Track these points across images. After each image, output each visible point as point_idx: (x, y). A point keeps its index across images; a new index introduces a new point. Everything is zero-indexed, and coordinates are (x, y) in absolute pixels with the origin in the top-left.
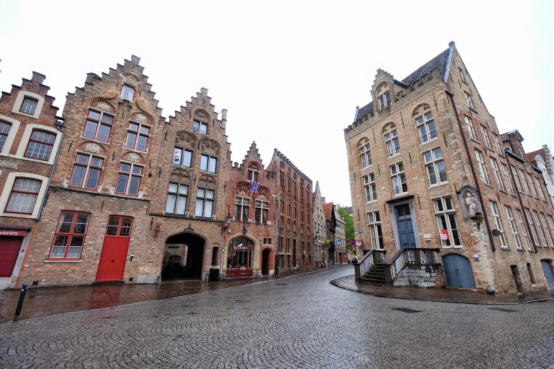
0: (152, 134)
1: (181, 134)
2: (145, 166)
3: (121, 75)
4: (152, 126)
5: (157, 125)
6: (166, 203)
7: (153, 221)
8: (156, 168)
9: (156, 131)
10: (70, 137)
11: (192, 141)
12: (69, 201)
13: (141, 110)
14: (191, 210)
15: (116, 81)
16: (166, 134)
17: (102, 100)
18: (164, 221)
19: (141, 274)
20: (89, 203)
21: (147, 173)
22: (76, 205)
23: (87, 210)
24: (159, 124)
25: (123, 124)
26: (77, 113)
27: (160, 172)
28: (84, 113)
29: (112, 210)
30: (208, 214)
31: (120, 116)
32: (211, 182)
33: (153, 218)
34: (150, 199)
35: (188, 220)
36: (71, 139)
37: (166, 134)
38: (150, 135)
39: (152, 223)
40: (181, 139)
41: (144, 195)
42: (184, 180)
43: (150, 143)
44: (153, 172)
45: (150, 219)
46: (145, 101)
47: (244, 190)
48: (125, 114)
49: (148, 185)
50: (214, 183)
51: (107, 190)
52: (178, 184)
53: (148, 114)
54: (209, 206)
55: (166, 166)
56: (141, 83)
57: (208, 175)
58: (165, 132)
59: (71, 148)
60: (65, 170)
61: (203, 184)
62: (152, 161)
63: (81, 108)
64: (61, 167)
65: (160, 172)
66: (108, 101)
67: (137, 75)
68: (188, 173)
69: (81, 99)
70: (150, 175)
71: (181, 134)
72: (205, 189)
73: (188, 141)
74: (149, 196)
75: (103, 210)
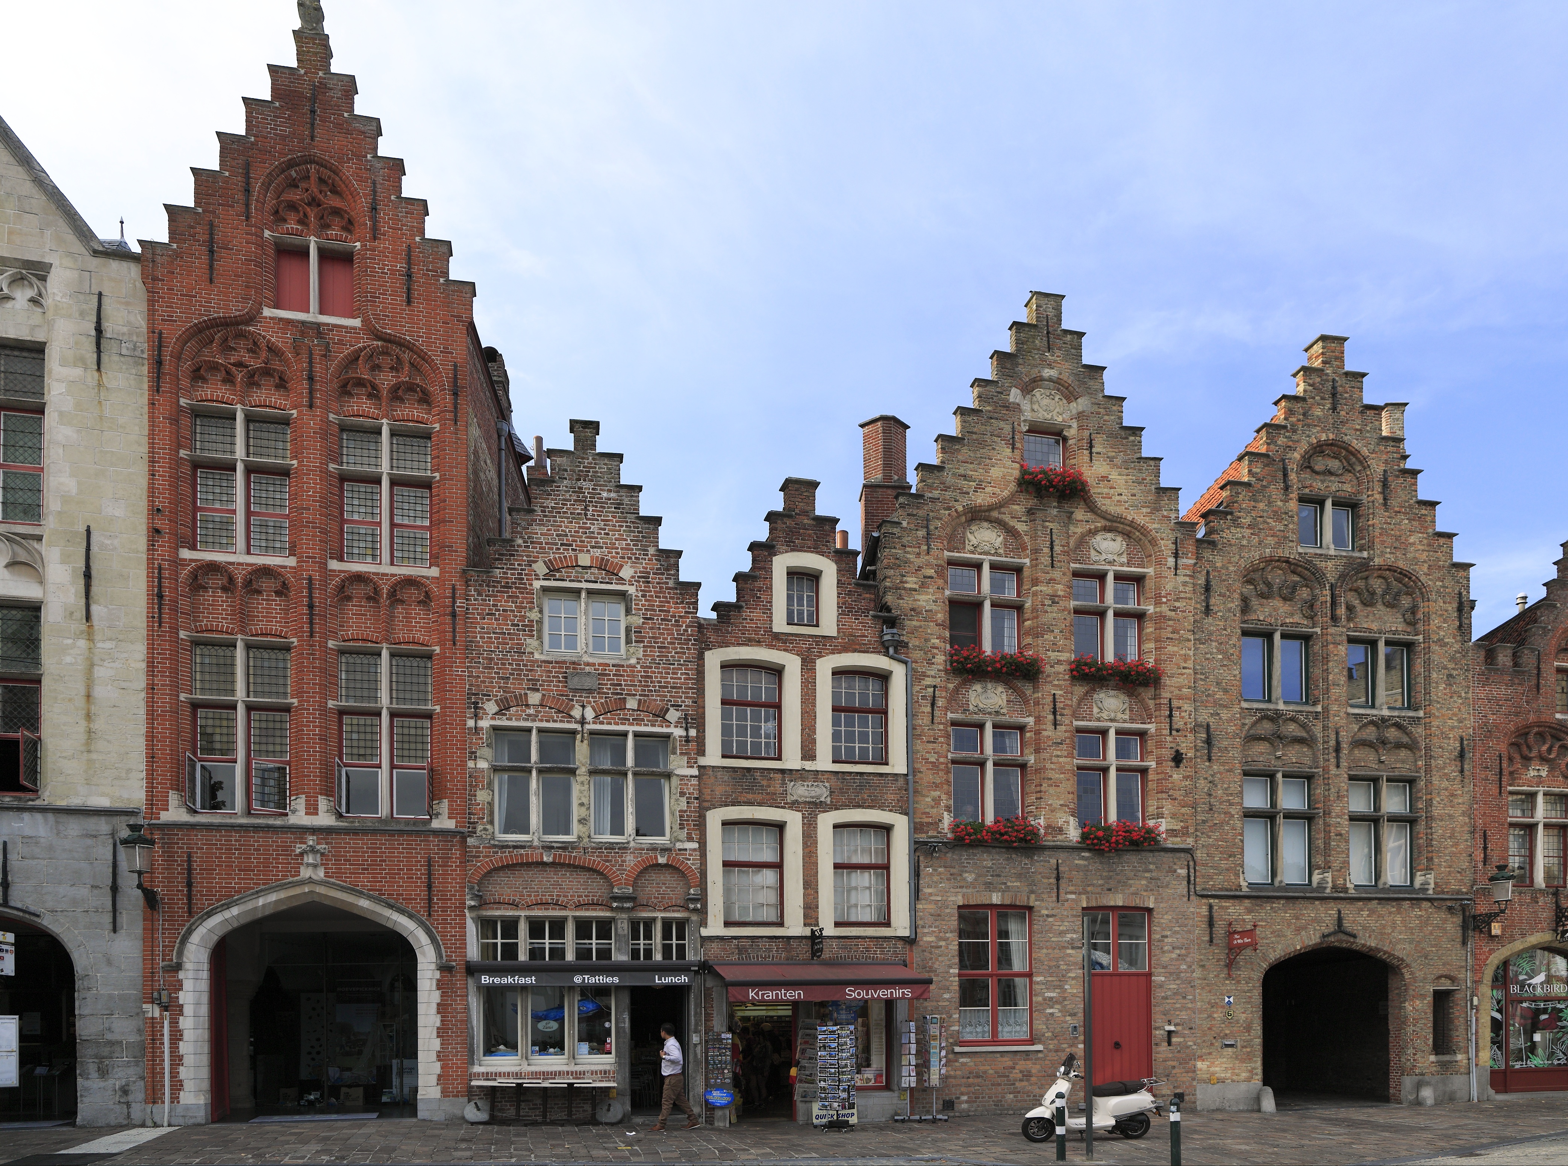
0: (1158, 603)
1: (1257, 576)
2: (1151, 727)
3: (1015, 396)
4: (1150, 571)
5: (1171, 561)
6: (1242, 853)
7: (1215, 915)
8: (1194, 730)
9: (1169, 587)
10: (924, 675)
11: (1304, 593)
12: (970, 877)
13: (1104, 515)
14: (1336, 865)
15: (1007, 428)
16: (1207, 588)
17: (976, 515)
18: (1249, 911)
20: (1019, 876)
21: (1168, 754)
22: (990, 887)
23: (1022, 901)
24: (1176, 555)
25: (1060, 589)
26: (923, 585)
27: (1209, 742)
28: (941, 582)
29: (1085, 892)
30: (1395, 873)
31: (1045, 560)
32: (1399, 746)
33: (1211, 907)
34: (1190, 842)
35: (1332, 904)
36: (928, 681)
37: (1207, 588)
38: (1151, 609)
39: (1211, 923)
40: (1262, 596)
42: (1294, 756)
43: (1157, 640)
44: (1187, 745)
45: (1204, 911)
46: (1114, 475)
47: (1543, 759)
48: (1057, 549)
49: (1177, 794)
50: (1412, 747)
51: (1060, 830)
52: (1272, 776)
53: (1132, 524)
54: (1395, 844)
55: (1225, 715)
56: (1082, 404)
57: (1383, 720)
58: (1202, 581)
59: (937, 713)
60: (936, 786)
61: (1368, 760)
62: (1175, 703)
63: (929, 565)
64: (927, 776)
65: (1209, 742)
66: (995, 514)
67: (1065, 377)
68: (1303, 726)
69: (921, 533)
70: (1178, 759)
71: (1257, 576)
72: (1375, 780)
73: (1285, 599)
74: (1184, 832)
75: (1062, 896)
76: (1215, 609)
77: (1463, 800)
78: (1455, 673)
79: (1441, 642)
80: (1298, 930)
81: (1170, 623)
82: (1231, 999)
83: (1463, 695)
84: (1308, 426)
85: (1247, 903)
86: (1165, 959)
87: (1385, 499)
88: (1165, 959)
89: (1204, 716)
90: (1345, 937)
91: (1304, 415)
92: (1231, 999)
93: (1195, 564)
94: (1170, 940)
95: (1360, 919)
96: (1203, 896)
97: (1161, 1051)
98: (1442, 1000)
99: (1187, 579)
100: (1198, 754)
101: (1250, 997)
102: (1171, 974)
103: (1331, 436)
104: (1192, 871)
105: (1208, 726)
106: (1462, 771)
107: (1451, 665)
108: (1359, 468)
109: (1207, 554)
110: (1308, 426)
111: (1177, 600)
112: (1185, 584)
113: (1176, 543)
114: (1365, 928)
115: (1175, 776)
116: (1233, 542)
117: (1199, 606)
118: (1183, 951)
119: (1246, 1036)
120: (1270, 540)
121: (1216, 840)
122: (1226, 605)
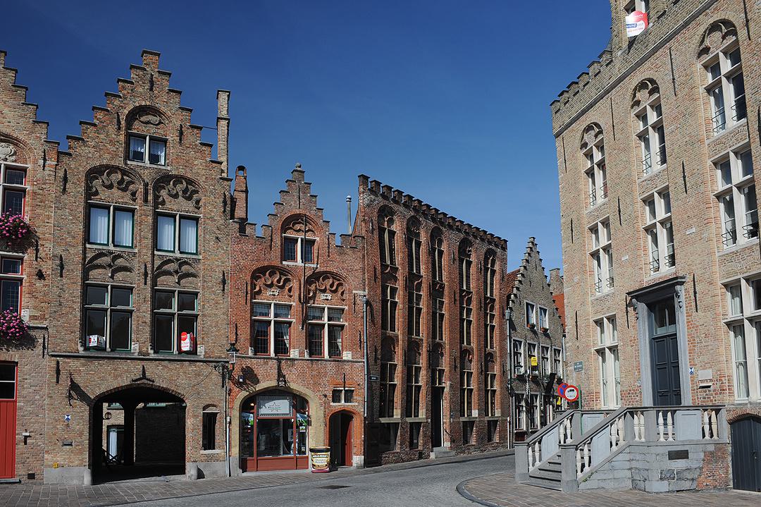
5: (41, 162)
18: (84, 365)
19: (49, 466)
21: (35, 272)
24: (45, 160)
33: (58, 362)
41: (33, 318)
44: (47, 267)
45: (53, 364)
49: (38, 295)
58: (61, 174)
70: (40, 275)
74: (43, 318)
76: (69, 191)
77: (225, 304)
78: (220, 236)
79: (212, 219)
80: (116, 377)
81: (38, 196)
82: (69, 417)
83: (225, 248)
84: (134, 96)
85: (82, 361)
86: (24, 392)
87: (180, 140)
88: (24, 392)
89: (59, 251)
90: (146, 381)
91: (132, 90)
92: (69, 417)
93: (56, 165)
94: (29, 381)
95: (157, 371)
96: (53, 356)
97: (20, 447)
98: (209, 422)
99: (51, 173)
100: (54, 272)
101: (83, 416)
102: (29, 401)
103: (148, 103)
104: (46, 340)
105: (61, 256)
106: (223, 290)
107: (217, 232)
108: (167, 122)
109: (65, 159)
110: (134, 96)
111: (44, 184)
112: (49, 175)
113: (44, 152)
114: (159, 377)
115: (38, 285)
116: (83, 155)
117: (58, 188)
118: (37, 388)
119: (79, 439)
120: (107, 156)
121: (63, 323)
122: (77, 189)
